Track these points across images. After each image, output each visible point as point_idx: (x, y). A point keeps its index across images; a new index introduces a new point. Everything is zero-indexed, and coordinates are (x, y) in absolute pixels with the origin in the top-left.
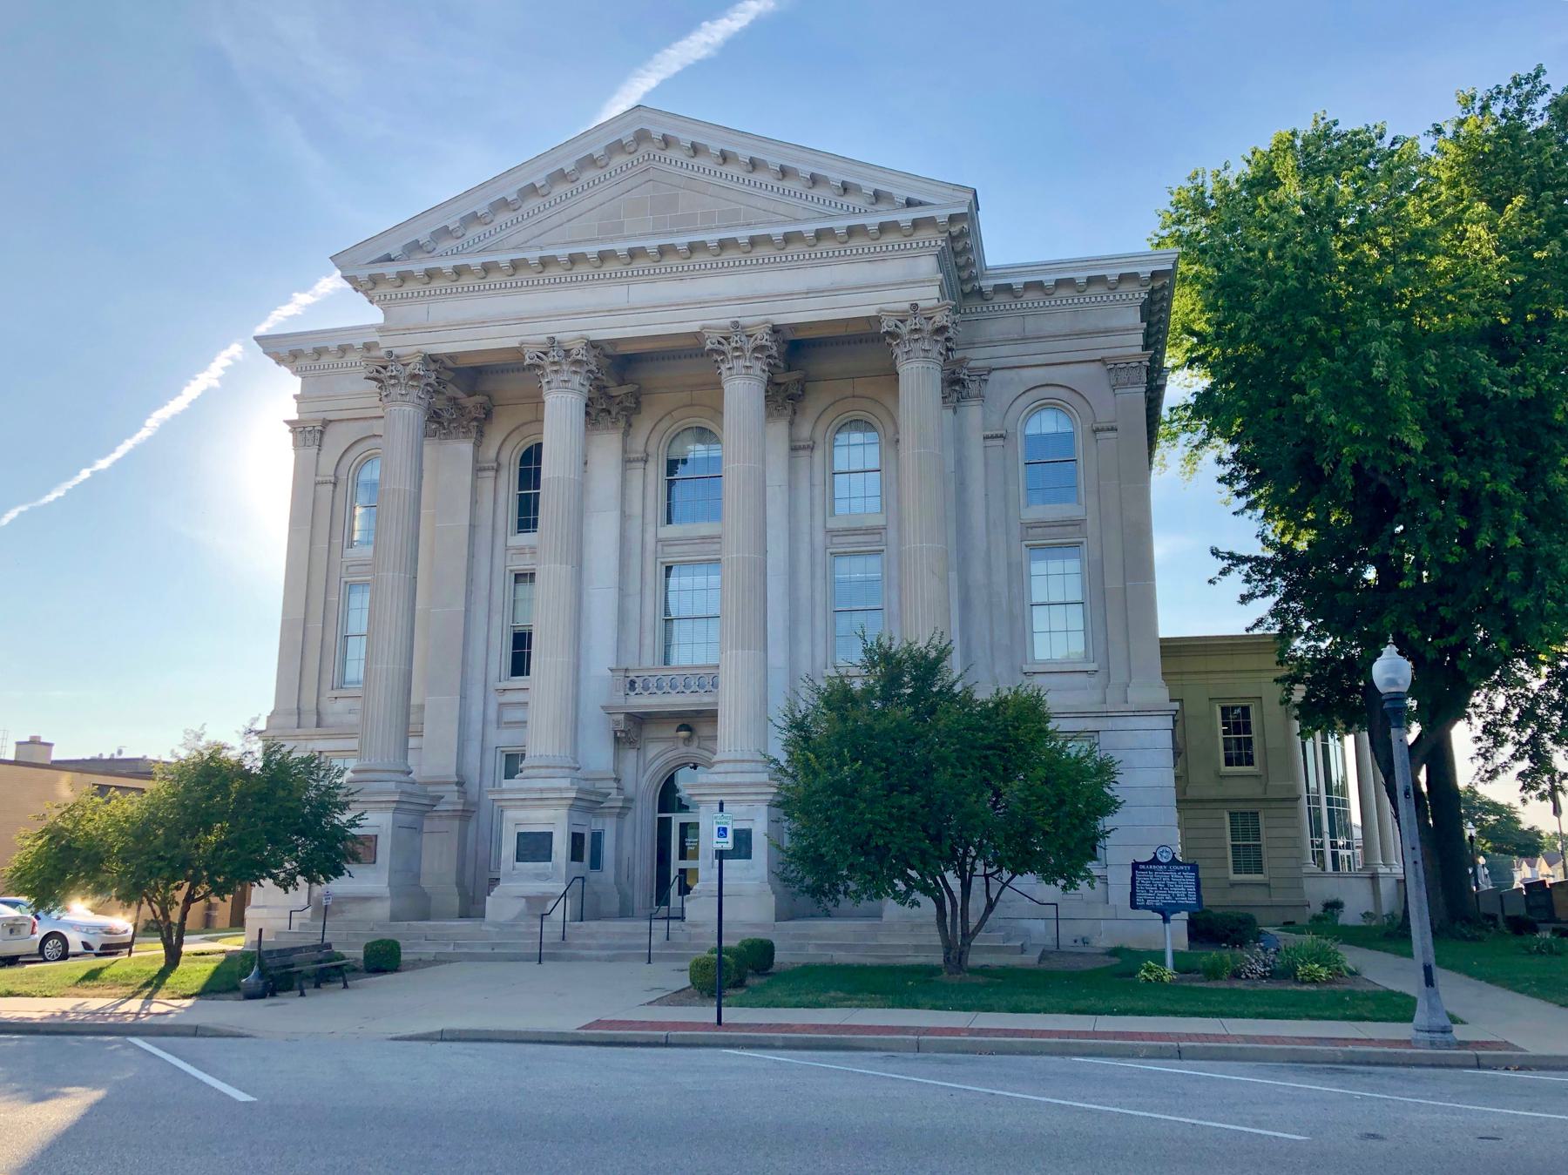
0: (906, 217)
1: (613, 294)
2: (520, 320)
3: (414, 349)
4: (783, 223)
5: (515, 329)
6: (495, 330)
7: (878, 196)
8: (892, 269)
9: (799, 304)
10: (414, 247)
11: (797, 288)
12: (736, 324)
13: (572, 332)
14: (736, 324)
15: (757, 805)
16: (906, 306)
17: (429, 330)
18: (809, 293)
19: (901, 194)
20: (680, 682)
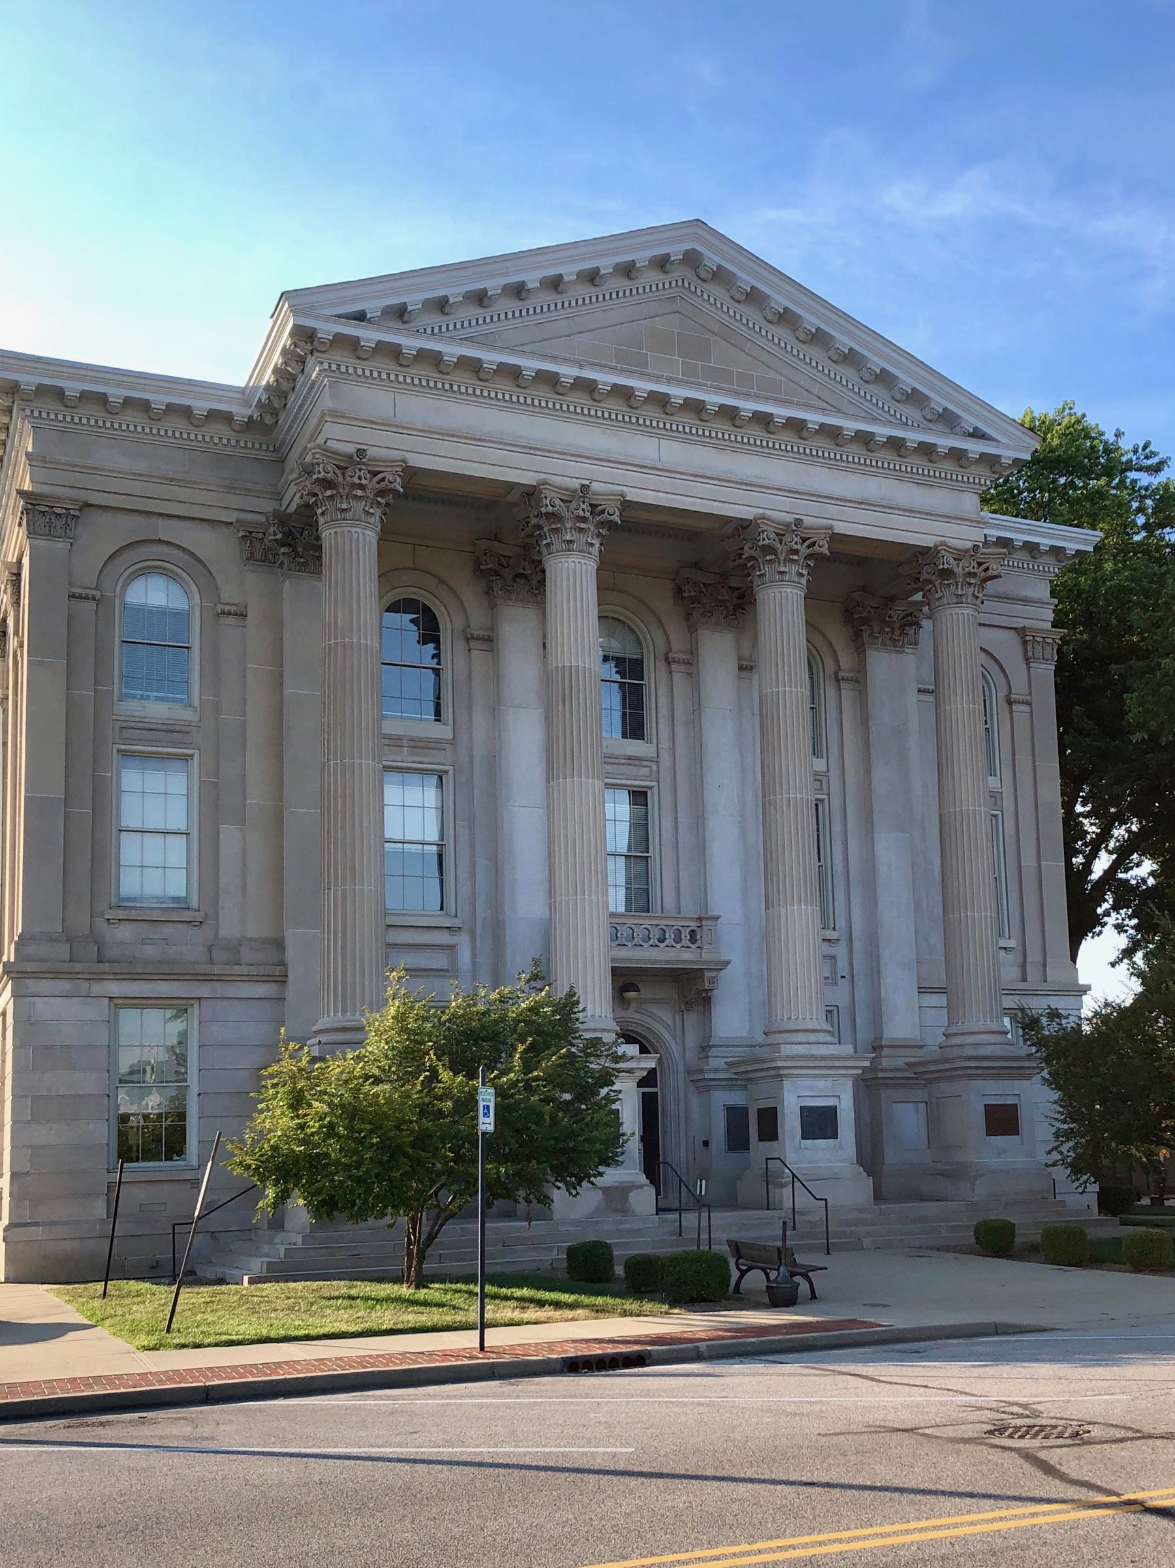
0: (975, 448)
1: (645, 447)
2: (530, 449)
3: (395, 455)
4: (857, 418)
5: (522, 459)
6: (493, 454)
7: (947, 419)
8: (938, 499)
9: (850, 512)
10: (400, 313)
11: (850, 496)
12: (798, 522)
13: (608, 482)
14: (798, 522)
15: (842, 1081)
16: (970, 545)
17: (399, 428)
18: (861, 503)
19: (970, 421)
20: (655, 934)
